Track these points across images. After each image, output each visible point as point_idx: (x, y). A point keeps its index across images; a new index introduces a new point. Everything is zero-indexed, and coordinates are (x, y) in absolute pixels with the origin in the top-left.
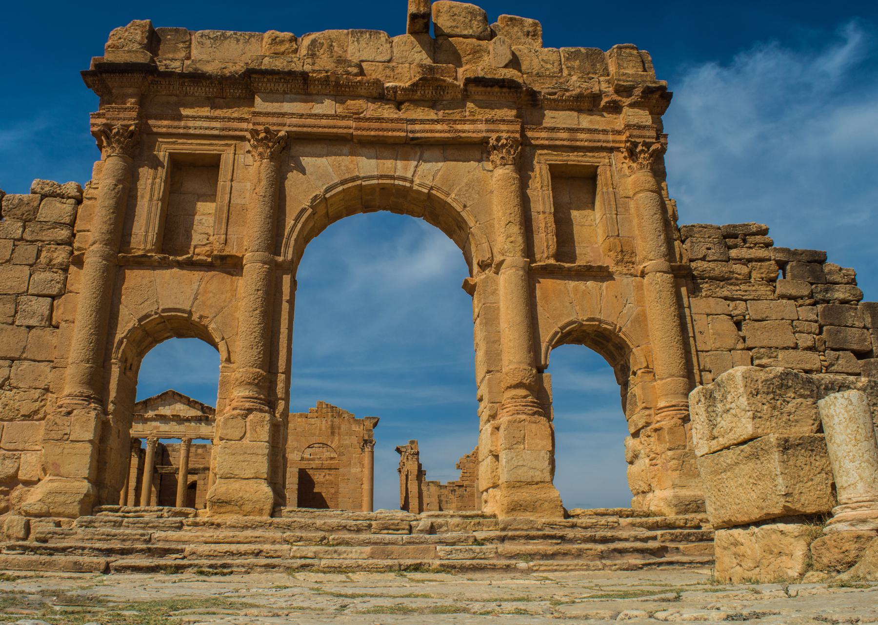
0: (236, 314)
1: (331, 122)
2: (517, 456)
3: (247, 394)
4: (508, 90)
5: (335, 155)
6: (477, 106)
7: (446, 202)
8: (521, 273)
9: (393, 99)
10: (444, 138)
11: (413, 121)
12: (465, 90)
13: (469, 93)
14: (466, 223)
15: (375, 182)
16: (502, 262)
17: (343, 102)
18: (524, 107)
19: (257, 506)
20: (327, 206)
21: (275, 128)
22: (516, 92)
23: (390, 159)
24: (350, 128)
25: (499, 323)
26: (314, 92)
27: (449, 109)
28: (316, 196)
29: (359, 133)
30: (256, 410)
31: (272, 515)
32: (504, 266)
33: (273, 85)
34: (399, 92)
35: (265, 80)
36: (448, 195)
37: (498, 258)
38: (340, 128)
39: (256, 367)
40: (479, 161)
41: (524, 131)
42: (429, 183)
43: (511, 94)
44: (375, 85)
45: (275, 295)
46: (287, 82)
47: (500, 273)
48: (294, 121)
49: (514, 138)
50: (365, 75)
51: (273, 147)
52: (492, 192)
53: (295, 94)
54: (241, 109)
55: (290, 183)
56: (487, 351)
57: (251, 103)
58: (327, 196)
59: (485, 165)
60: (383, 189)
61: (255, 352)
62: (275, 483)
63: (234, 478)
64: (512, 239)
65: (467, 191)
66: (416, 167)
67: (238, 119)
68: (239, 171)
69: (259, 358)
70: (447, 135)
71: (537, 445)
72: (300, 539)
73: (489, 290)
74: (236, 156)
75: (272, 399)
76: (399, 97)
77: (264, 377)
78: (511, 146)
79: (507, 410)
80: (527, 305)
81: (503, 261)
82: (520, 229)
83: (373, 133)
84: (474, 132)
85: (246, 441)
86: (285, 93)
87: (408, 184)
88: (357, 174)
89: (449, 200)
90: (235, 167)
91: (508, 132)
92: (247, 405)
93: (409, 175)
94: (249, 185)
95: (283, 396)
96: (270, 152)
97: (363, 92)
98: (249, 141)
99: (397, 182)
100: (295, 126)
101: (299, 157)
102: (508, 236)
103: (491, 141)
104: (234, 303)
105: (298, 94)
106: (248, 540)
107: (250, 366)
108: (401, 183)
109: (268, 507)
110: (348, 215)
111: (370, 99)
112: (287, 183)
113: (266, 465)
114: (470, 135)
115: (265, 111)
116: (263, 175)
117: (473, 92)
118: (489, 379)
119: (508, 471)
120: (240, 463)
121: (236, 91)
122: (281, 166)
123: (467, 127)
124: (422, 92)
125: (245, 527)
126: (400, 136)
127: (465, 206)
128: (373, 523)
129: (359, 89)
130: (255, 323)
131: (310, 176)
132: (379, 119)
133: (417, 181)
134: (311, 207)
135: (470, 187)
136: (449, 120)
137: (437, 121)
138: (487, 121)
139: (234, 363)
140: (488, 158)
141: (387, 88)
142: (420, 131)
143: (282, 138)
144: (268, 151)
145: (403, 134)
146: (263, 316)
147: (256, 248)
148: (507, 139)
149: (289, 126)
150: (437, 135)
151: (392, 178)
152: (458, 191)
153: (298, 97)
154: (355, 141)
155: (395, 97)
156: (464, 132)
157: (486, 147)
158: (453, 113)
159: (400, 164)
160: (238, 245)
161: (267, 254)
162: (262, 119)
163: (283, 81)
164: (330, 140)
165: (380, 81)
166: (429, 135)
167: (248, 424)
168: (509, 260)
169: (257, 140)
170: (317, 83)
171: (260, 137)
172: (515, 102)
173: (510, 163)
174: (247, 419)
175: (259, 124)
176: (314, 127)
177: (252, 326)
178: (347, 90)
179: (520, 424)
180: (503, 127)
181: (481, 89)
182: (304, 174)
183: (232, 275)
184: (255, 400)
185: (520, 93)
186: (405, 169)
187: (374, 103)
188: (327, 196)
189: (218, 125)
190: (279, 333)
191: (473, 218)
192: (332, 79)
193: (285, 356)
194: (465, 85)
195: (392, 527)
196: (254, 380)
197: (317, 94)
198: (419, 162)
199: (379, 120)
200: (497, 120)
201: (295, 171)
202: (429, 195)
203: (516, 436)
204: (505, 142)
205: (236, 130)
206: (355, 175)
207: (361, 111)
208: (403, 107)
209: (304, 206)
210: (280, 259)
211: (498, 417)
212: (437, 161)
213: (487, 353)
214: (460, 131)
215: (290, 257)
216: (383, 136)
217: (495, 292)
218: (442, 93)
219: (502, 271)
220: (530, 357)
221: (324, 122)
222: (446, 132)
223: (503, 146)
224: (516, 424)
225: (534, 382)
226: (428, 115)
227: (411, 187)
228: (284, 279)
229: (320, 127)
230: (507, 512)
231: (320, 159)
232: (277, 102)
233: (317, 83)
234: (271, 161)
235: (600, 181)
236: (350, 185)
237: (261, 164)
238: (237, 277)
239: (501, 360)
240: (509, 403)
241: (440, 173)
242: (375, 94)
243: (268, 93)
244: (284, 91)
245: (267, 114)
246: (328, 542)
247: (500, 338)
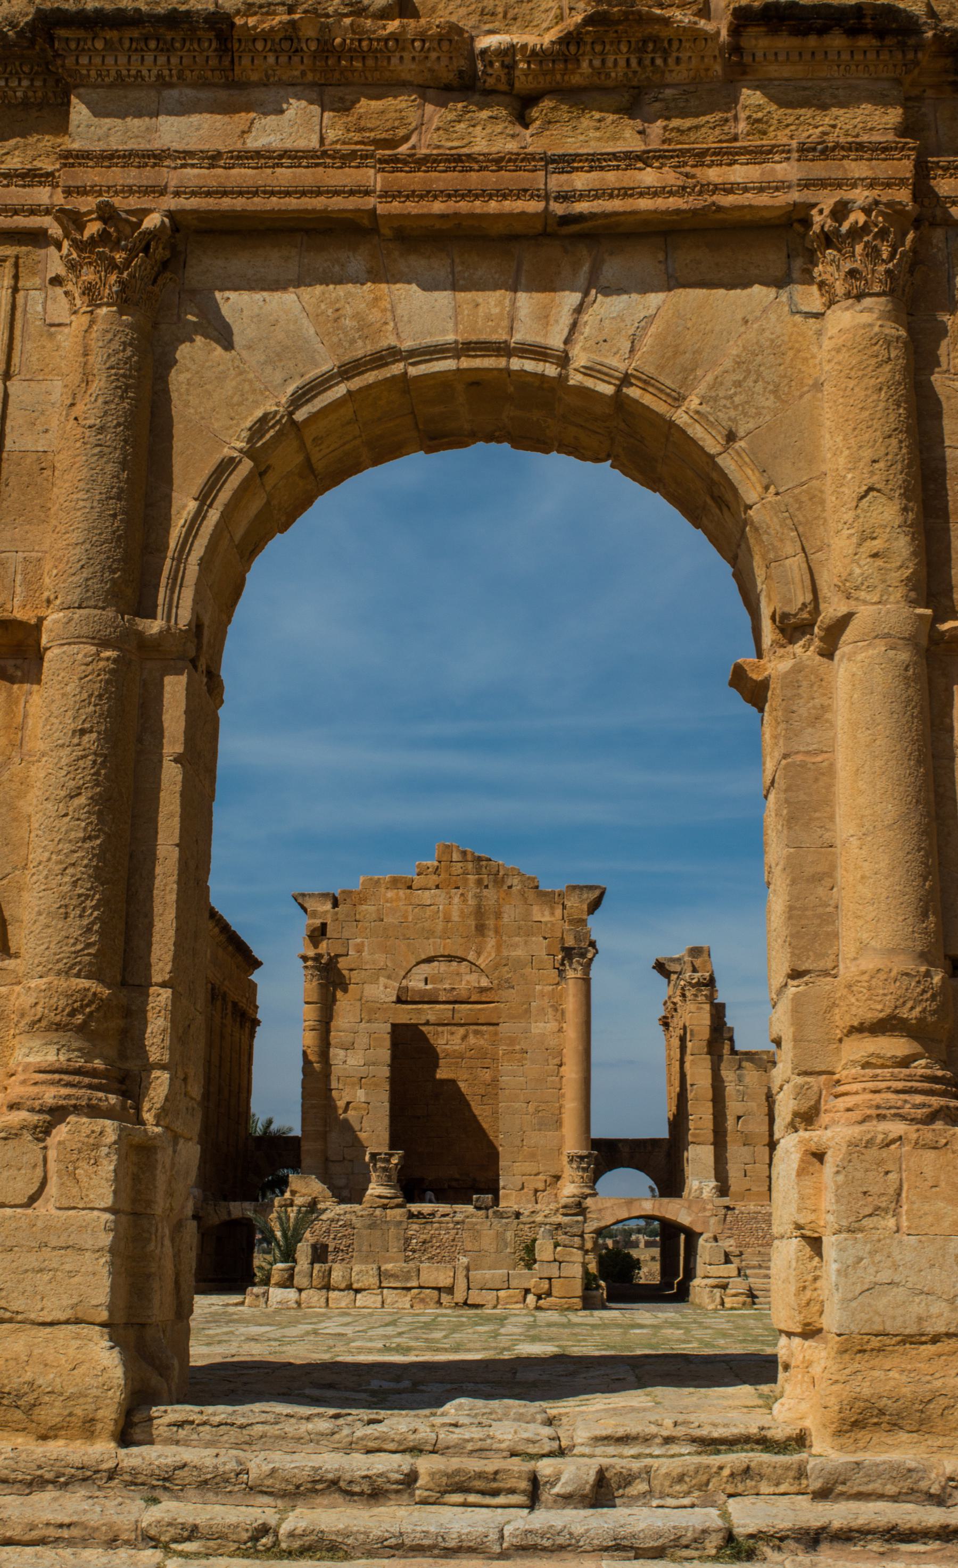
0: (21, 803)
1: (306, 176)
2: (872, 1253)
3: (51, 1058)
4: (875, 42)
5: (326, 279)
6: (772, 98)
7: (671, 424)
8: (904, 656)
9: (503, 87)
10: (667, 212)
12: (736, 49)
13: (747, 59)
14: (735, 490)
15: (449, 364)
16: (844, 621)
17: (344, 107)
18: (930, 93)
19: (78, 1411)
20: (303, 445)
21: (134, 202)
22: (903, 46)
23: (496, 287)
24: (367, 193)
25: (832, 818)
26: (255, 77)
27: (683, 115)
28: (264, 419)
29: (396, 207)
30: (76, 1109)
31: (125, 1439)
32: (849, 634)
33: (122, 60)
34: (523, 65)
35: (99, 45)
36: (678, 399)
37: (833, 608)
38: (337, 193)
39: (78, 976)
40: (780, 283)
41: (927, 177)
42: (618, 363)
43: (885, 56)
44: (445, 46)
45: (140, 740)
46: (168, 49)
47: (838, 654)
48: (193, 175)
49: (889, 204)
50: (415, 14)
51: (127, 263)
52: (818, 386)
53: (194, 85)
54: (31, 140)
55: (183, 377)
56: (791, 908)
57: (61, 126)
58: (300, 415)
59: (797, 298)
60: (476, 384)
61: (75, 927)
62: (143, 1325)
63: (10, 1321)
64: (877, 545)
65: (738, 384)
66: (579, 310)
67: (23, 176)
68: (29, 346)
69: (88, 945)
70: (673, 203)
71: (939, 1218)
72: (192, 1533)
73: (803, 711)
74: (20, 296)
75: (132, 1065)
76: (522, 84)
77: (104, 1006)
78: (883, 234)
79: (849, 1101)
80: (919, 762)
81: (847, 618)
82: (905, 509)
83: (438, 207)
84: (761, 190)
85: (46, 1209)
86: (163, 83)
87: (551, 370)
88: (392, 341)
89: (681, 417)
90: (18, 332)
91: (872, 183)
92: (50, 1095)
93: (555, 341)
94: (57, 390)
95: (166, 1058)
96: (120, 282)
97: (406, 68)
98: (59, 246)
99: (516, 364)
100: (194, 194)
101: (211, 291)
102: (866, 537)
103: (817, 219)
104: (15, 768)
105: (203, 84)
106: (35, 1534)
107: (59, 973)
108: (530, 366)
109: (109, 1414)
110: (376, 462)
111: (430, 93)
112: (178, 379)
113: (107, 1282)
114: (749, 199)
115: (97, 147)
116: (97, 361)
117: (759, 55)
118: (796, 998)
119: (846, 1301)
120: (30, 1275)
121: (14, 83)
122: (155, 325)
123: (739, 173)
124: (597, 63)
125: (36, 1483)
126: (523, 213)
127: (731, 437)
128: (425, 1465)
129: (395, 61)
130: (73, 835)
131: (244, 354)
132: (458, 159)
133: (580, 357)
134: (250, 453)
135: (748, 372)
136: (683, 152)
137: (644, 159)
138: (805, 151)
139: (17, 956)
140: (809, 272)
141: (484, 52)
143: (153, 235)
144: (113, 278)
145: (535, 206)
146: (100, 814)
147: (75, 597)
148: (867, 211)
149: (177, 194)
150: (644, 204)
151: (503, 349)
152: (711, 387)
153: (204, 94)
154: (386, 231)
155: (511, 84)
156: (729, 189)
157: (804, 236)
158: (697, 128)
159: (526, 301)
160: (27, 583)
161: (110, 613)
162: (91, 176)
163: (153, 44)
164: (307, 232)
165: (460, 31)
166: (616, 205)
167: (52, 1154)
168: (865, 614)
169: (78, 245)
170: (259, 45)
171: (87, 234)
172: (898, 81)
173: (877, 289)
174: (50, 1141)
175: (82, 191)
176: (256, 194)
177: (67, 847)
178: (357, 64)
179: (884, 1153)
180: (858, 169)
181: (785, 42)
182: (228, 345)
183: (12, 680)
184: (77, 1078)
185: (917, 48)
186: (544, 318)
187: (444, 105)
188: (300, 415)
190: (151, 857)
191: (754, 476)
192: (309, 32)
193: (172, 933)
194: (735, 31)
195: (479, 1484)
196: (72, 1014)
197: (264, 84)
198: (586, 294)
199: (458, 161)
200: (837, 146)
201: (199, 339)
202: (619, 401)
203: (874, 1189)
204: (861, 218)
205: (16, 213)
206: (384, 344)
207: (401, 132)
208: (535, 113)
209: (226, 452)
210: (154, 627)
211: (824, 1118)
212: (645, 288)
213: (792, 912)
214: (717, 188)
215: (185, 616)
216: (472, 216)
217: (820, 717)
218: (659, 62)
219: (844, 649)
220: (925, 932)
221: (285, 175)
222: (671, 193)
223: (856, 233)
224: (873, 1152)
225: (934, 1012)
226: (614, 138)
227: (562, 379)
228: (167, 689)
229: (273, 193)
230: (839, 1433)
231: (277, 295)
232: (139, 115)
233: (259, 45)
234: (121, 312)
236: (371, 377)
237: (92, 322)
238: (26, 686)
239: (836, 935)
240: (855, 1080)
241: (652, 330)
242: (448, 76)
243: (111, 86)
244: (159, 76)
245: (108, 158)
246: (276, 1543)
247: (833, 867)
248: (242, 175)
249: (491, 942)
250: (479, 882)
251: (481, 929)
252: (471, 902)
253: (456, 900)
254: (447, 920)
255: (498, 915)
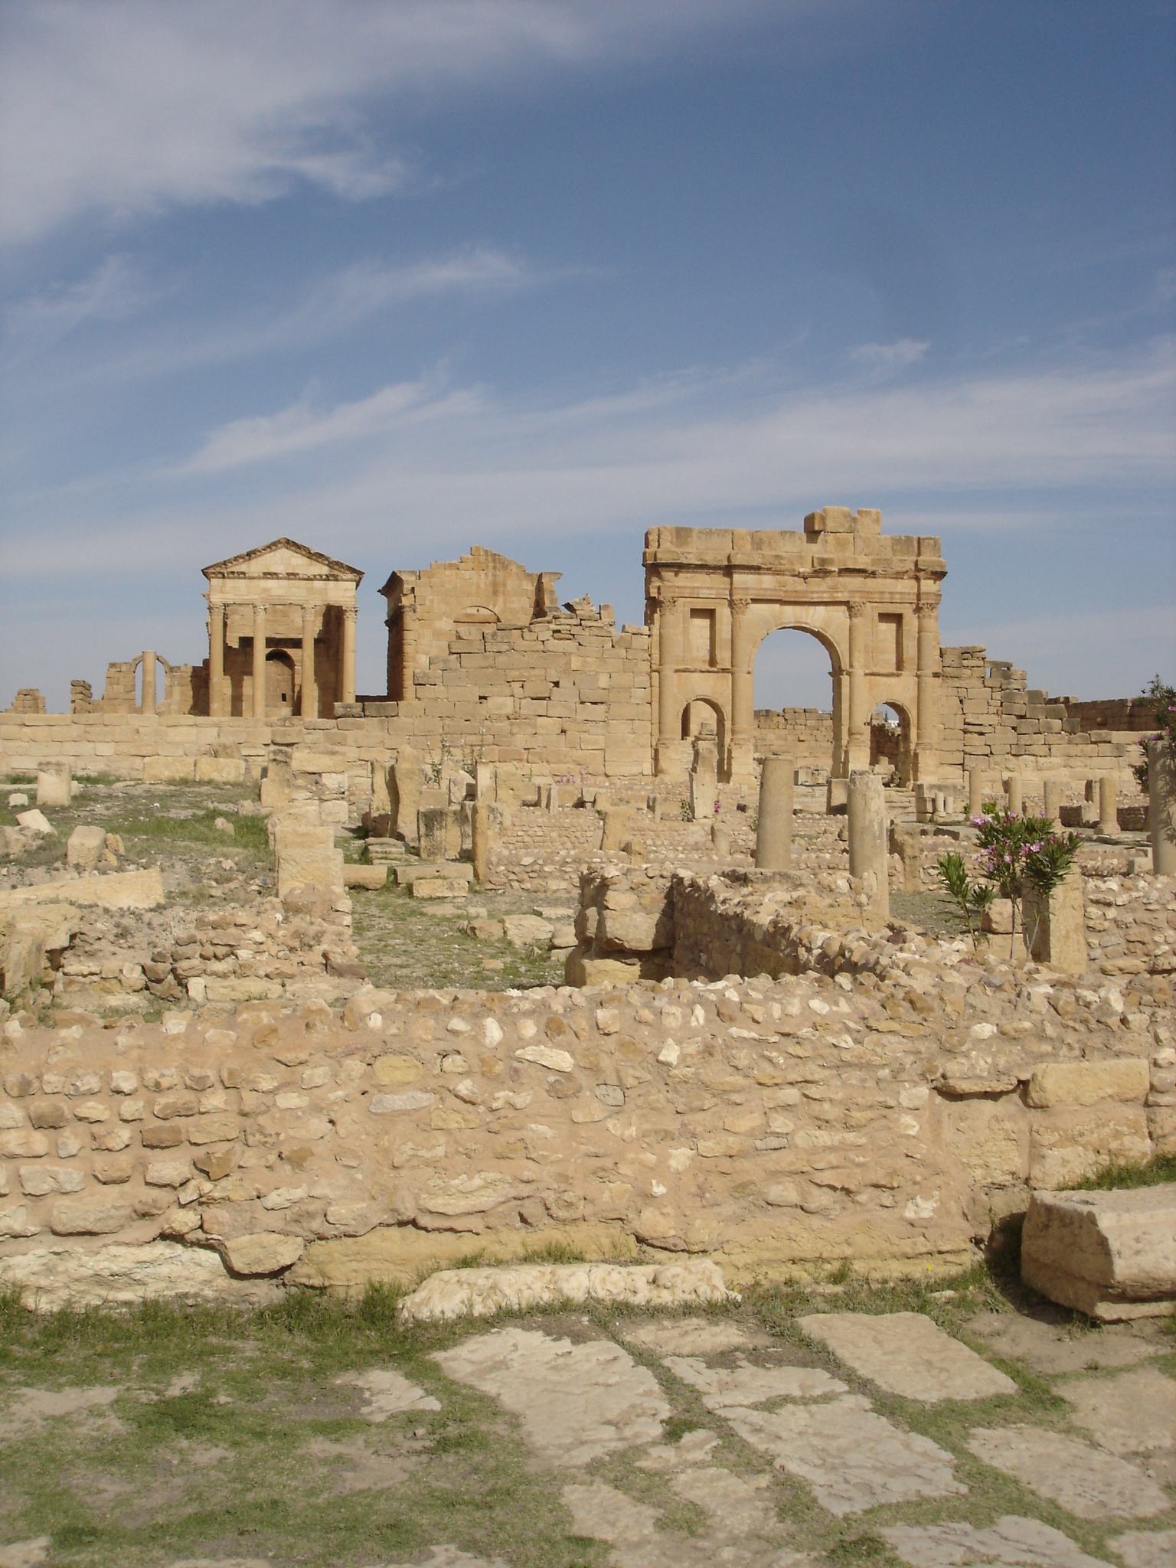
11: (812, 592)
123: (839, 595)
142: (815, 598)
180: (857, 595)
189: (714, 592)
235: (904, 621)
248: (762, 592)
249: (501, 599)
250: (495, 568)
251: (495, 593)
252: (490, 578)
253: (483, 576)
254: (478, 587)
255: (505, 585)
